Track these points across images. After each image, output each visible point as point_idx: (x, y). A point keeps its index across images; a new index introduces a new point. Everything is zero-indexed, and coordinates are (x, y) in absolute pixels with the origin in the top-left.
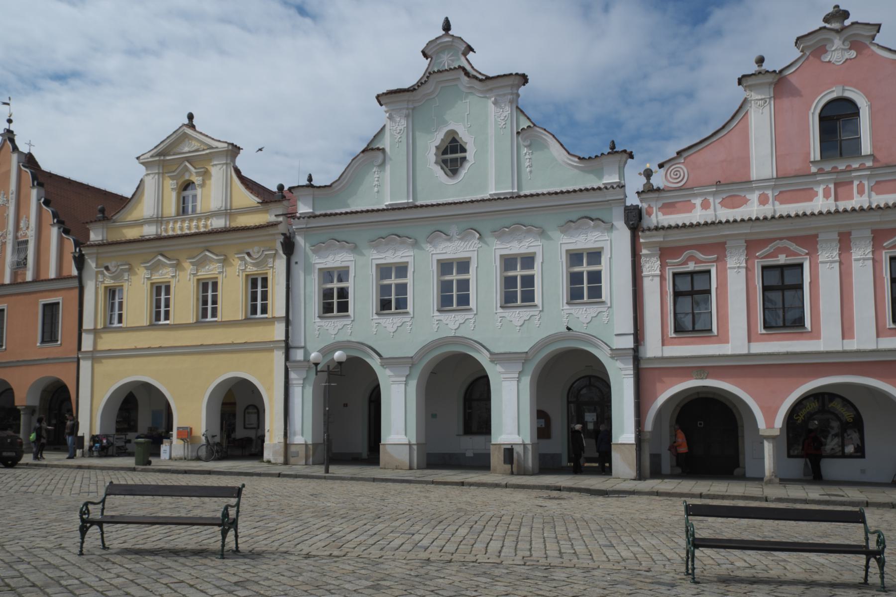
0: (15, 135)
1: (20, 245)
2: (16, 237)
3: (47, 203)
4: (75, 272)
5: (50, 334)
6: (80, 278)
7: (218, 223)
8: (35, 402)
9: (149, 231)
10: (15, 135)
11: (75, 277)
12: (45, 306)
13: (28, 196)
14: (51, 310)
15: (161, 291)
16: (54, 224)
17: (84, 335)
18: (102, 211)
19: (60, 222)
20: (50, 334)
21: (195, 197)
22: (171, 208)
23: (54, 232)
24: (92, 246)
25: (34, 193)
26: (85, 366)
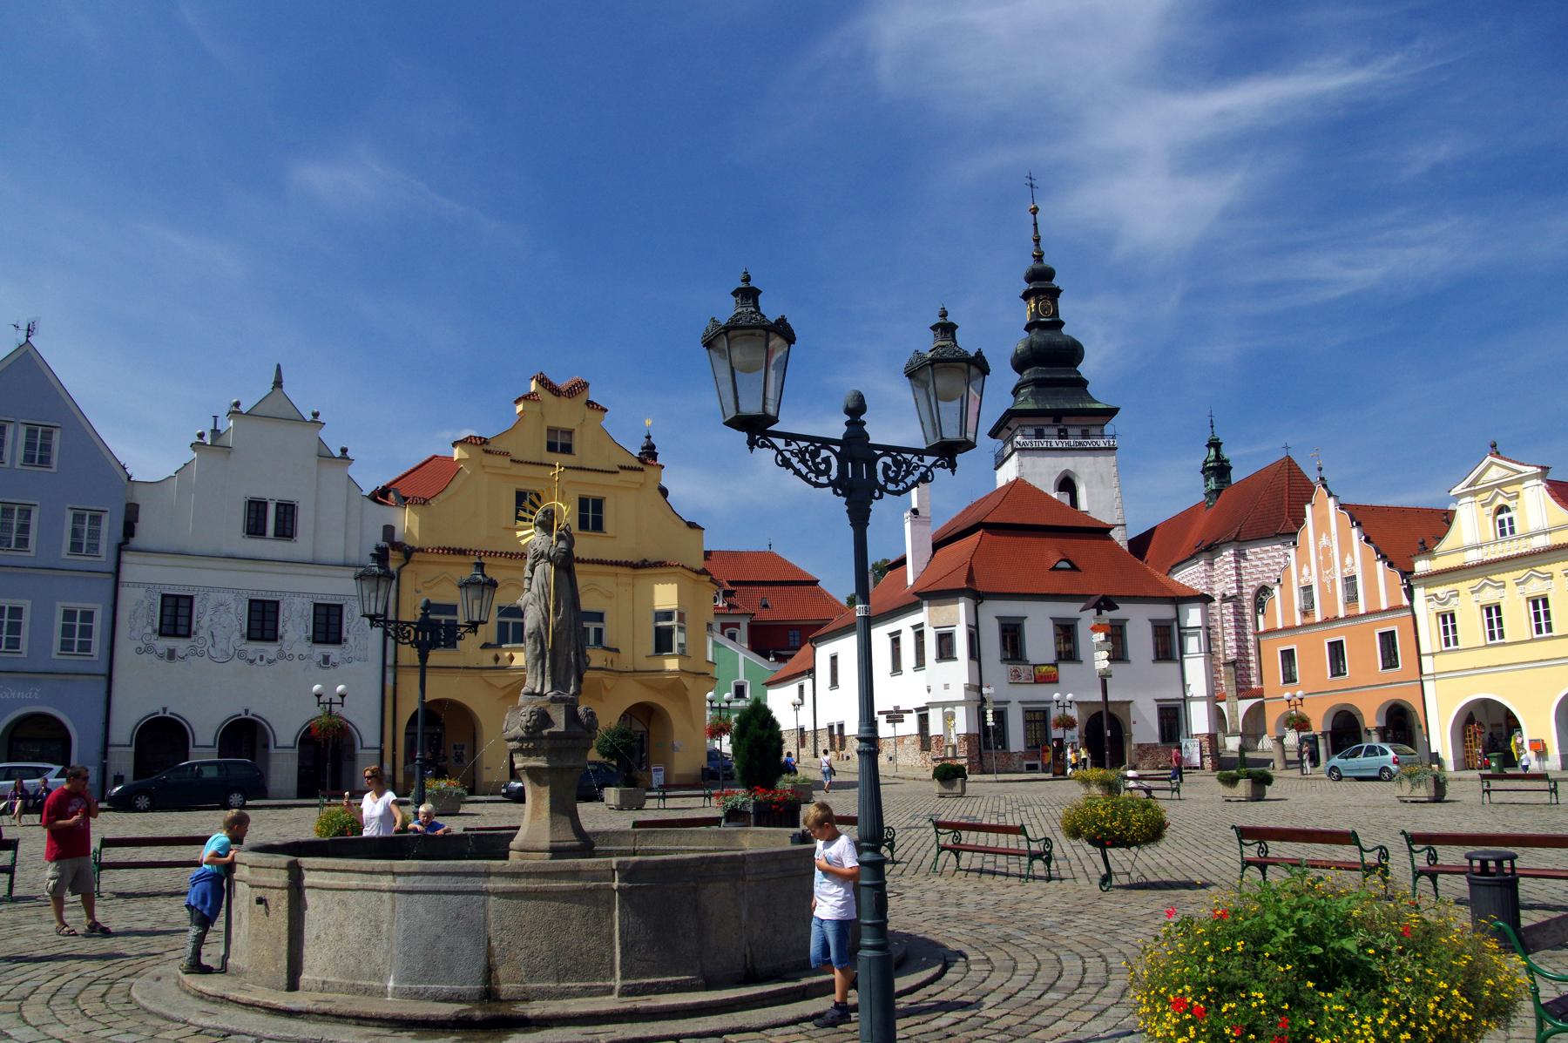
1: (1350, 581)
2: (1342, 574)
3: (1367, 540)
4: (1406, 602)
5: (1390, 659)
6: (1411, 608)
7: (1540, 542)
8: (1383, 724)
9: (1473, 557)
11: (1407, 607)
12: (1381, 635)
13: (1350, 536)
14: (1388, 639)
15: (1493, 612)
16: (1378, 560)
17: (1423, 658)
18: (1423, 543)
19: (1384, 557)
20: (1390, 659)
21: (1511, 520)
22: (1490, 531)
23: (1380, 564)
24: (1420, 577)
25: (1355, 531)
26: (1428, 686)
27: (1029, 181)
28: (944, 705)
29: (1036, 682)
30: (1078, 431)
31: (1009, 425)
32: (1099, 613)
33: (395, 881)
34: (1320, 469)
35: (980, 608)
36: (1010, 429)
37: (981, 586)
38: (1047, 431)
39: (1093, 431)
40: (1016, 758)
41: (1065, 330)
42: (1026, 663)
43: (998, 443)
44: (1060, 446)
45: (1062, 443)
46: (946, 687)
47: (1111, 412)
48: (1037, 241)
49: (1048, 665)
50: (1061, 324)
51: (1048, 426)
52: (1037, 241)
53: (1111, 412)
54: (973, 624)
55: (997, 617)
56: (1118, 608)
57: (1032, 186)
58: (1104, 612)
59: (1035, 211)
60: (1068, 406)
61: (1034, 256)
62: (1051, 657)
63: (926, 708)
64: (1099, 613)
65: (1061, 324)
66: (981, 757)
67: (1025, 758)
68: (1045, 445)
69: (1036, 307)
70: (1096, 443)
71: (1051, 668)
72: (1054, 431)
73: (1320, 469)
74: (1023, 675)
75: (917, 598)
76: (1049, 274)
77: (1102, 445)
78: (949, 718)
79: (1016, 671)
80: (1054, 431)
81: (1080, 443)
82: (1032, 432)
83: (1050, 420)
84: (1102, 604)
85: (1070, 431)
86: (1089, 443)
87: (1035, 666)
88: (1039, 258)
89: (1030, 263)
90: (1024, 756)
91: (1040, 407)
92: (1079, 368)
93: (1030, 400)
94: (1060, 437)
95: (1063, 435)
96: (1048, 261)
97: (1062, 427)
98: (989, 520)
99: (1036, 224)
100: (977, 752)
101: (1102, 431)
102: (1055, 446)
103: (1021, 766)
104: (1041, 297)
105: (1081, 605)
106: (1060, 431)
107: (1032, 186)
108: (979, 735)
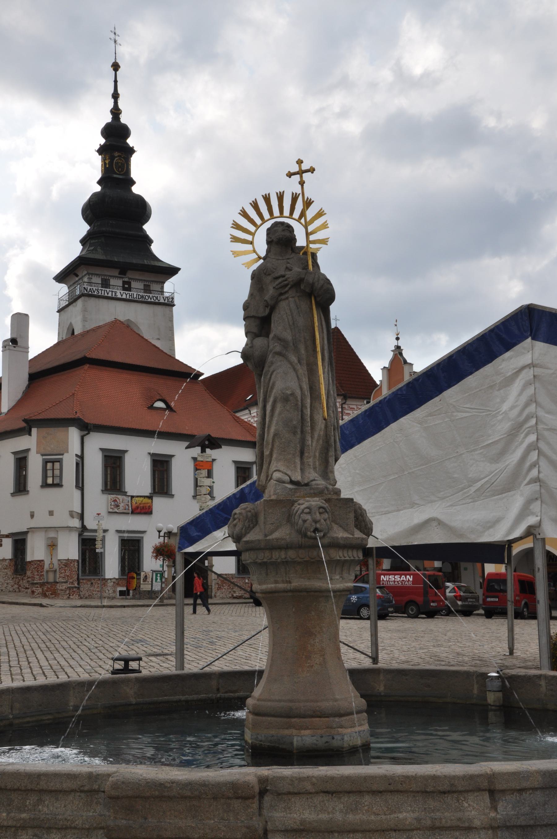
0: (402, 350)
10: (402, 350)
27: (112, 36)
28: (46, 529)
29: (133, 513)
30: (140, 285)
31: (76, 272)
32: (203, 451)
33: (494, 808)
34: (398, 339)
35: (86, 439)
36: (77, 276)
37: (90, 419)
38: (113, 282)
39: (154, 287)
40: (110, 584)
41: (135, 189)
42: (125, 493)
43: (63, 289)
44: (124, 296)
45: (125, 295)
46: (51, 513)
47: (172, 271)
48: (116, 96)
49: (144, 497)
50: (133, 183)
51: (111, 276)
52: (116, 96)
53: (172, 271)
54: (79, 454)
55: (101, 449)
56: (220, 447)
57: (115, 42)
58: (208, 450)
59: (116, 67)
60: (134, 261)
61: (112, 112)
62: (147, 490)
63: (26, 533)
64: (203, 451)
65: (133, 183)
66: (78, 584)
67: (118, 584)
68: (110, 295)
69: (111, 163)
70: (157, 298)
71: (147, 500)
72: (119, 282)
73: (398, 339)
74: (122, 505)
75: (24, 425)
76: (125, 132)
77: (162, 301)
78: (52, 546)
79: (115, 501)
80: (119, 282)
81: (142, 297)
82: (99, 280)
83: (116, 272)
84: (207, 443)
85: (134, 284)
86: (150, 297)
87: (132, 497)
88: (116, 112)
89: (109, 118)
90: (117, 582)
91: (109, 258)
92: (146, 227)
93: (99, 250)
94: (124, 289)
95: (127, 287)
96: (124, 119)
97: (126, 280)
98: (94, 356)
99: (116, 82)
100: (76, 578)
101: (163, 288)
102: (119, 296)
103: (114, 592)
104: (116, 154)
105: (187, 444)
106: (124, 282)
107: (115, 42)
108: (78, 561)
